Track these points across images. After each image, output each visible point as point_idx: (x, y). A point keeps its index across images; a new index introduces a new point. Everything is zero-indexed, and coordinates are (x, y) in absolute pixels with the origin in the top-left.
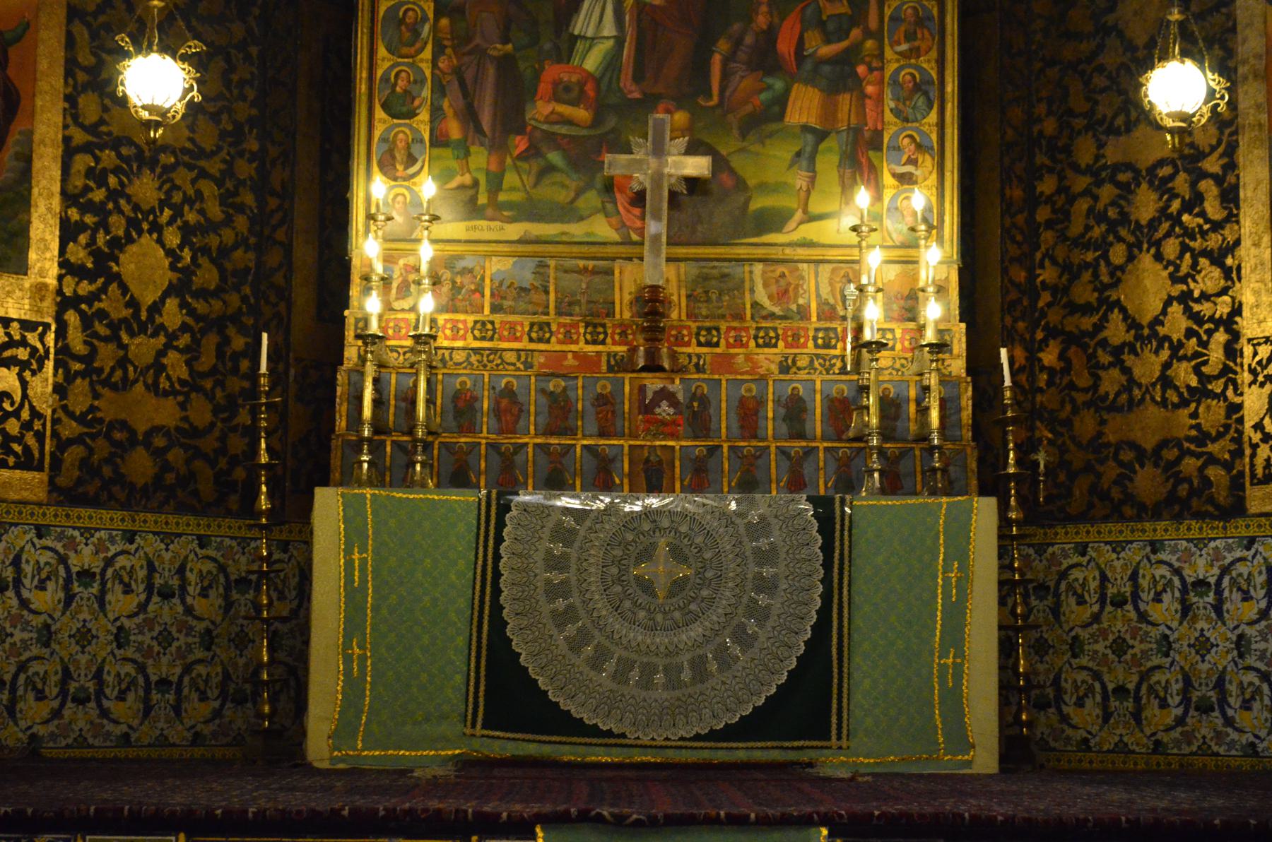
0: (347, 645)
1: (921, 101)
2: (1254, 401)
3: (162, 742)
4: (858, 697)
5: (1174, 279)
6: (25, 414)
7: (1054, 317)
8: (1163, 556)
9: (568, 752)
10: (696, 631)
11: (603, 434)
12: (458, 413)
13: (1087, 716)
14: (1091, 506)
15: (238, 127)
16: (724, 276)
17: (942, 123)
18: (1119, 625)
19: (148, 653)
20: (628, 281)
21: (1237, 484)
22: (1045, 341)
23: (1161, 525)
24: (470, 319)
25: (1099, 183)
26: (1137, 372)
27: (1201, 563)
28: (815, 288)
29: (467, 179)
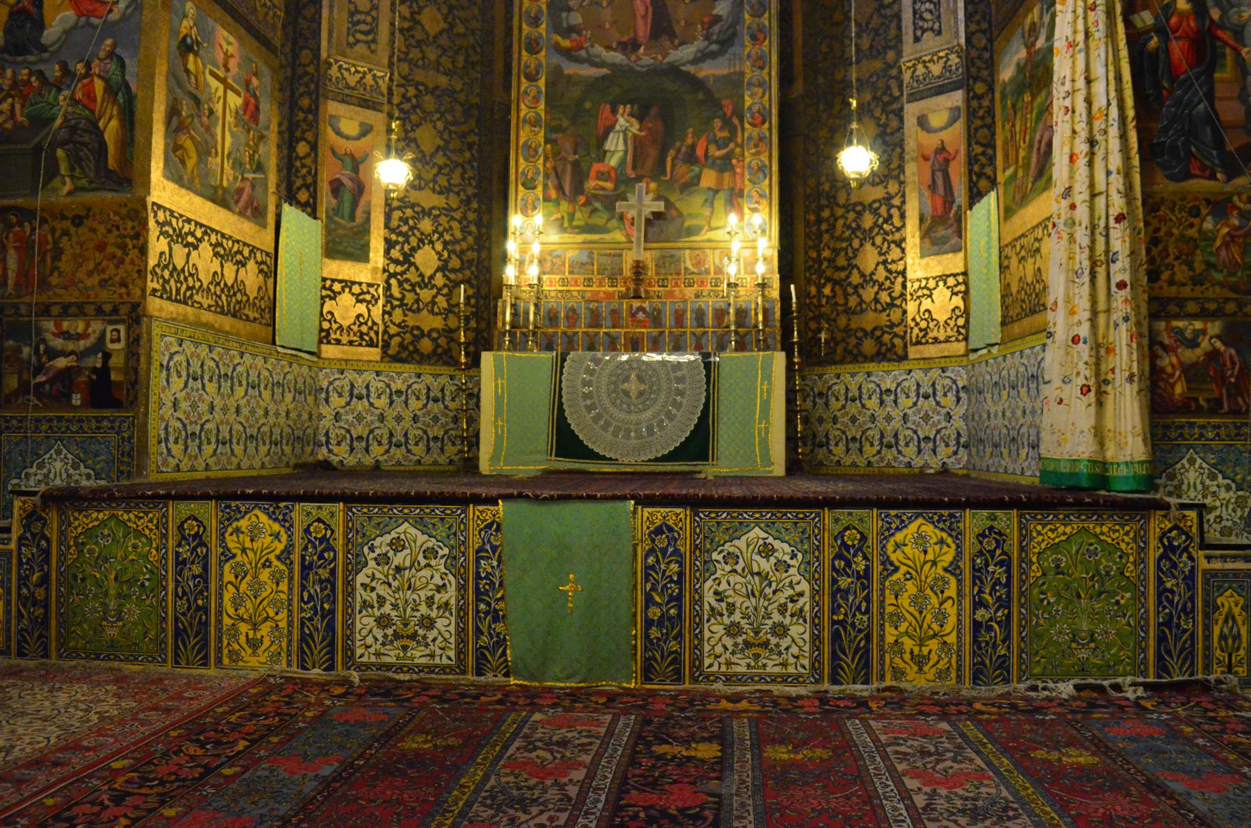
0: (496, 420)
1: (761, 175)
2: (911, 307)
3: (435, 463)
4: (722, 442)
6: (370, 323)
7: (828, 273)
8: (872, 378)
9: (592, 467)
10: (649, 414)
11: (614, 327)
12: (550, 319)
13: (839, 450)
14: (844, 357)
15: (468, 198)
16: (672, 256)
17: (770, 185)
19: (428, 425)
20: (629, 259)
21: (905, 346)
24: (558, 277)
25: (848, 212)
26: (864, 297)
28: (712, 259)
29: (559, 216)
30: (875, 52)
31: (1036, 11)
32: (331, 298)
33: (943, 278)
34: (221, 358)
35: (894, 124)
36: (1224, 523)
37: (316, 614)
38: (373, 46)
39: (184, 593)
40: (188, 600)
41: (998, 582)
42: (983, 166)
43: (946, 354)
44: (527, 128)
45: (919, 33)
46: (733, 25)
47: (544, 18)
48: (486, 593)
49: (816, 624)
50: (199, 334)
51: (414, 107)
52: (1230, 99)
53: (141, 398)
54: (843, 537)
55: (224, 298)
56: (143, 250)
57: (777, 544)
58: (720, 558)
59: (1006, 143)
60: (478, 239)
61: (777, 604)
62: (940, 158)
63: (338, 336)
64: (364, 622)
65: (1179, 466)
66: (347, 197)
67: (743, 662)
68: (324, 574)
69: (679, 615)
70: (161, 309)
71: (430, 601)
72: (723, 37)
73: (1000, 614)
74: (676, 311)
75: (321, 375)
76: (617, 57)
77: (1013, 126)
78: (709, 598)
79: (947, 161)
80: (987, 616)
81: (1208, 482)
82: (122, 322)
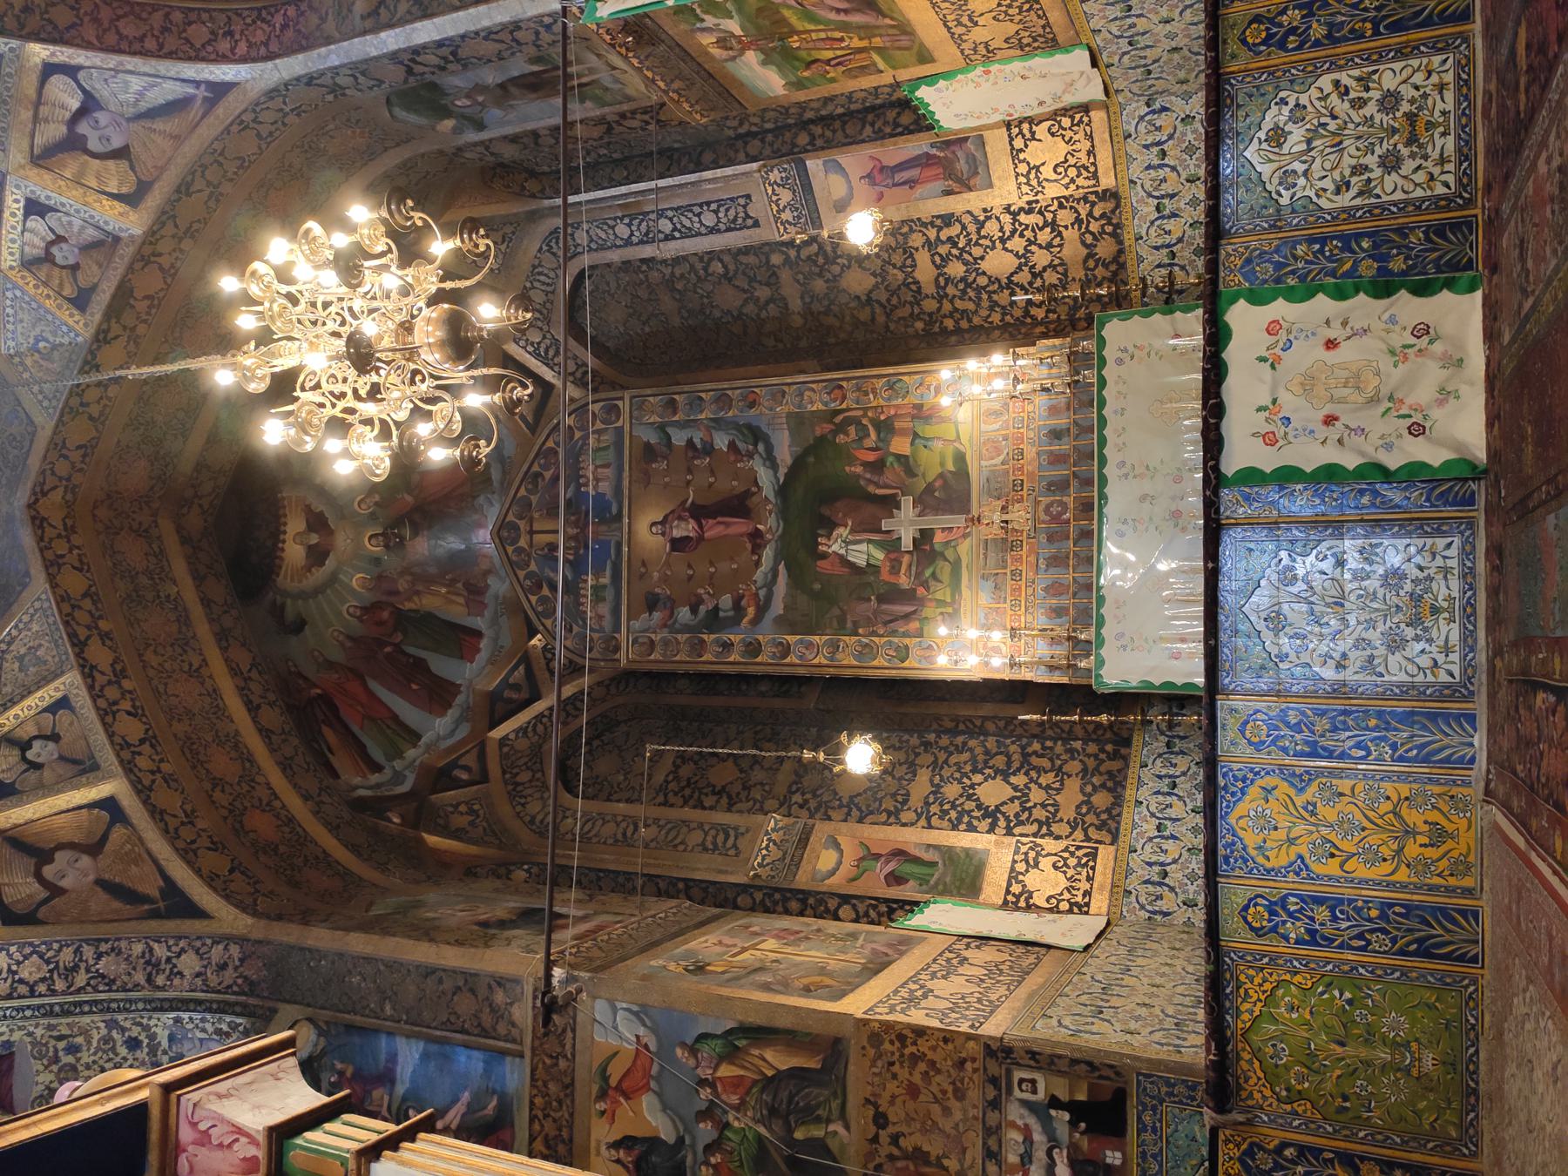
2: (1053, 191)
5: (993, 248)
6: (1066, 855)
8: (1144, 233)
18: (1186, 253)
22: (1032, 317)
23: (1126, 236)
25: (946, 295)
27: (1146, 210)
30: (773, 280)
31: (707, 40)
33: (1015, 154)
38: (742, 830)
39: (1360, 936)
42: (886, 123)
43: (1107, 136)
44: (839, 656)
45: (750, 222)
47: (725, 637)
49: (1381, 56)
51: (815, 796)
54: (1254, 45)
57: (1268, 124)
59: (850, 74)
60: (971, 734)
61: (1351, 112)
66: (908, 868)
70: (998, 1025)
76: (768, 554)
77: (828, 62)
78: (1345, 200)
79: (882, 169)
82: (1009, 1073)
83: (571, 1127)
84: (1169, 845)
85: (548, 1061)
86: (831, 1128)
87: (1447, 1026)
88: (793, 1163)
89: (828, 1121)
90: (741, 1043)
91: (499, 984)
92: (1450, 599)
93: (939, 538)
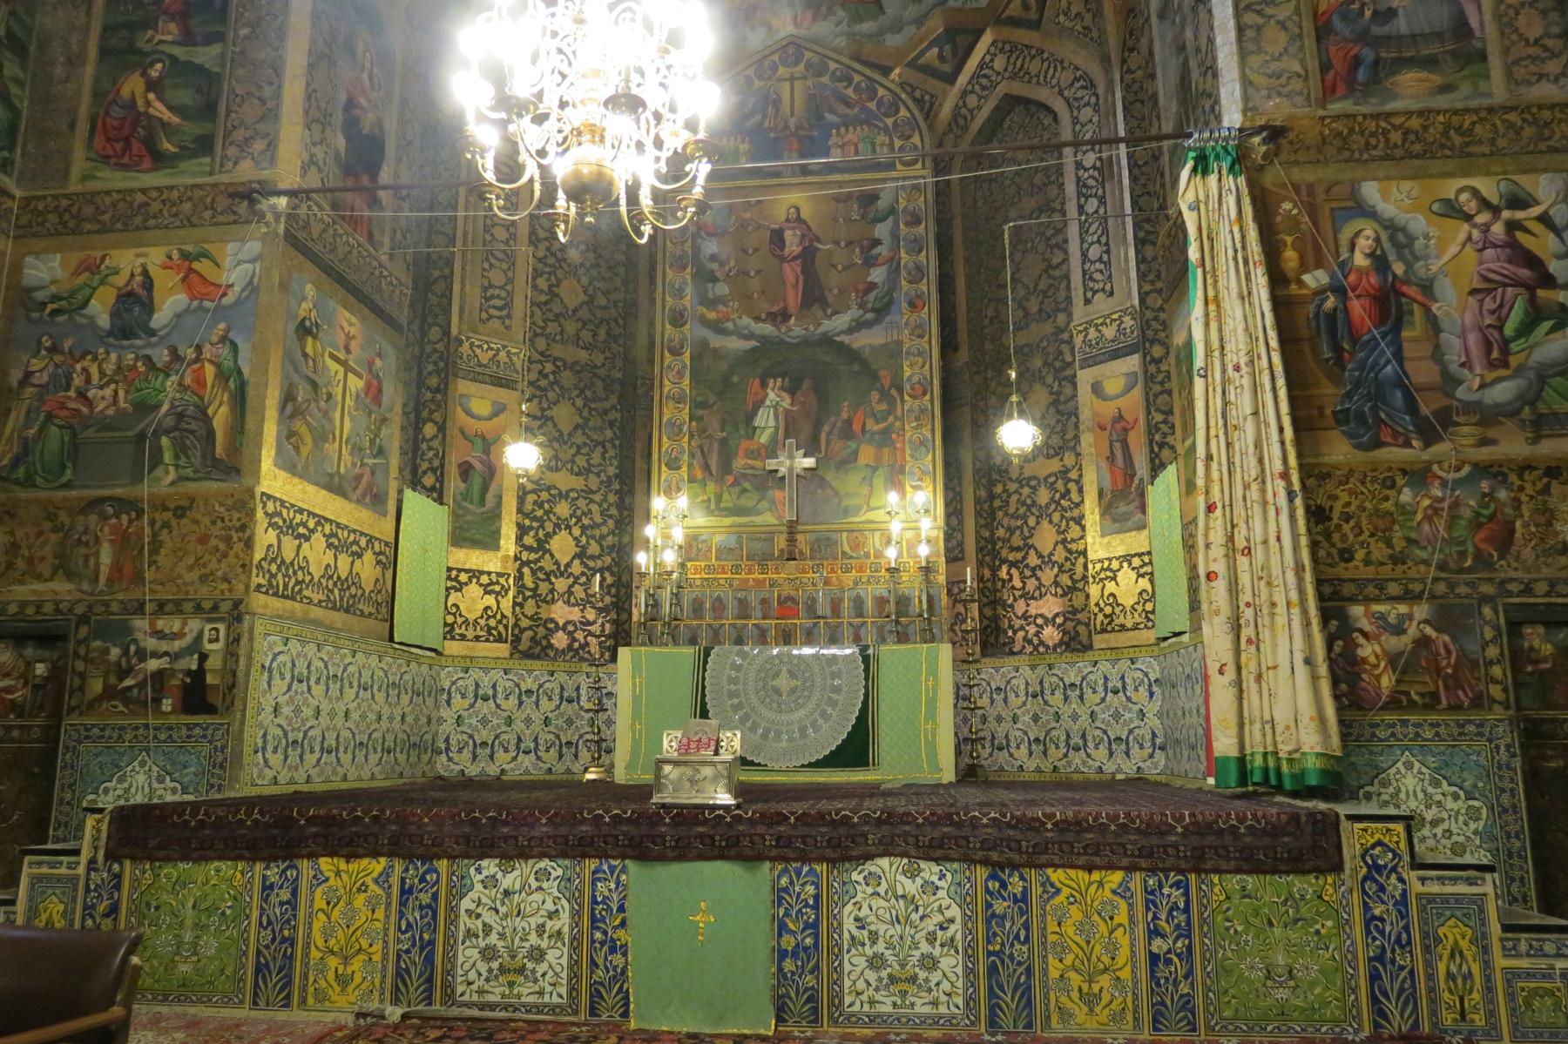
0: (633, 724)
2: (1094, 590)
10: (802, 713)
11: (764, 618)
12: (695, 611)
15: (609, 478)
17: (932, 459)
19: (561, 729)
30: (1044, 315)
32: (457, 590)
33: (1127, 558)
34: (331, 658)
35: (1068, 391)
36: (1455, 838)
37: (414, 945)
39: (270, 923)
40: (273, 931)
41: (1175, 907)
44: (671, 404)
46: (889, 292)
48: (603, 920)
49: (969, 954)
50: (306, 632)
51: (552, 384)
52: (1420, 359)
53: (238, 704)
55: (336, 592)
56: (249, 544)
58: (860, 878)
59: (1183, 412)
60: (619, 523)
61: (923, 933)
62: (1118, 427)
63: (463, 631)
64: (468, 955)
65: (1393, 771)
66: (477, 482)
67: (888, 1001)
68: (425, 898)
69: (816, 945)
70: (266, 606)
71: (541, 929)
72: (878, 305)
73: (1179, 944)
74: (832, 601)
75: (443, 674)
76: (767, 329)
78: (849, 925)
79: (1126, 430)
80: (1165, 948)
81: (1430, 790)
83: (157, 227)
84: (513, 701)
85: (209, 200)
86: (171, 469)
87: (210, 982)
88: (142, 436)
89: (177, 466)
90: (232, 384)
91: (269, 145)
92: (519, 996)
93: (777, 494)
